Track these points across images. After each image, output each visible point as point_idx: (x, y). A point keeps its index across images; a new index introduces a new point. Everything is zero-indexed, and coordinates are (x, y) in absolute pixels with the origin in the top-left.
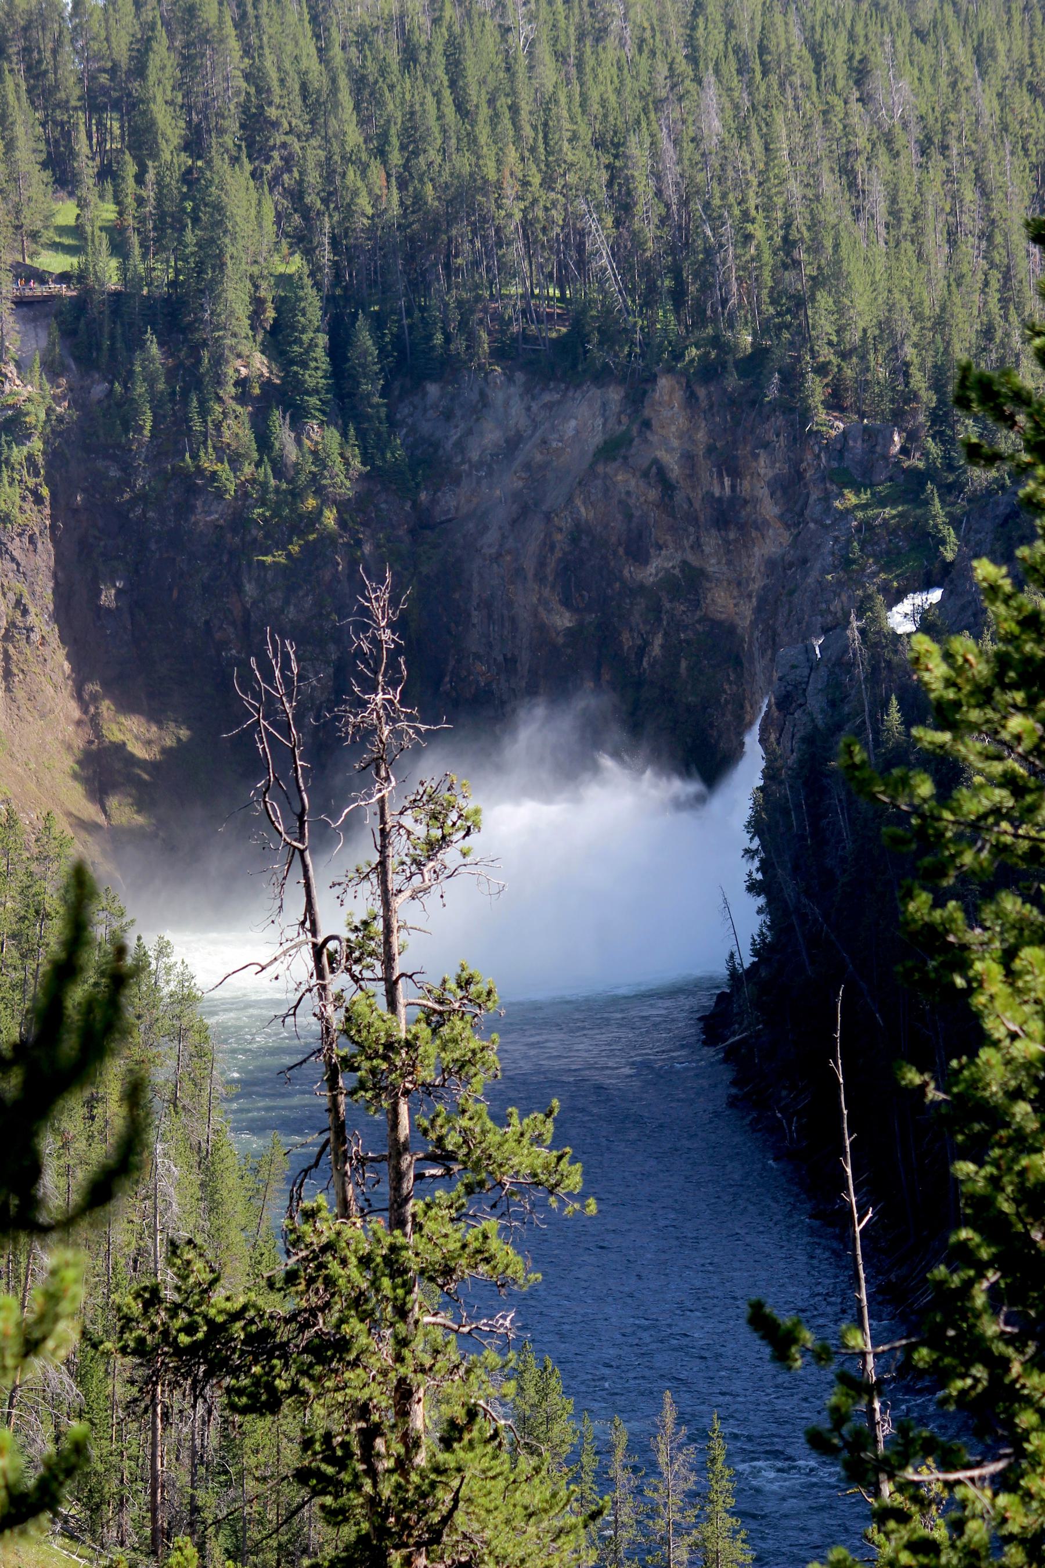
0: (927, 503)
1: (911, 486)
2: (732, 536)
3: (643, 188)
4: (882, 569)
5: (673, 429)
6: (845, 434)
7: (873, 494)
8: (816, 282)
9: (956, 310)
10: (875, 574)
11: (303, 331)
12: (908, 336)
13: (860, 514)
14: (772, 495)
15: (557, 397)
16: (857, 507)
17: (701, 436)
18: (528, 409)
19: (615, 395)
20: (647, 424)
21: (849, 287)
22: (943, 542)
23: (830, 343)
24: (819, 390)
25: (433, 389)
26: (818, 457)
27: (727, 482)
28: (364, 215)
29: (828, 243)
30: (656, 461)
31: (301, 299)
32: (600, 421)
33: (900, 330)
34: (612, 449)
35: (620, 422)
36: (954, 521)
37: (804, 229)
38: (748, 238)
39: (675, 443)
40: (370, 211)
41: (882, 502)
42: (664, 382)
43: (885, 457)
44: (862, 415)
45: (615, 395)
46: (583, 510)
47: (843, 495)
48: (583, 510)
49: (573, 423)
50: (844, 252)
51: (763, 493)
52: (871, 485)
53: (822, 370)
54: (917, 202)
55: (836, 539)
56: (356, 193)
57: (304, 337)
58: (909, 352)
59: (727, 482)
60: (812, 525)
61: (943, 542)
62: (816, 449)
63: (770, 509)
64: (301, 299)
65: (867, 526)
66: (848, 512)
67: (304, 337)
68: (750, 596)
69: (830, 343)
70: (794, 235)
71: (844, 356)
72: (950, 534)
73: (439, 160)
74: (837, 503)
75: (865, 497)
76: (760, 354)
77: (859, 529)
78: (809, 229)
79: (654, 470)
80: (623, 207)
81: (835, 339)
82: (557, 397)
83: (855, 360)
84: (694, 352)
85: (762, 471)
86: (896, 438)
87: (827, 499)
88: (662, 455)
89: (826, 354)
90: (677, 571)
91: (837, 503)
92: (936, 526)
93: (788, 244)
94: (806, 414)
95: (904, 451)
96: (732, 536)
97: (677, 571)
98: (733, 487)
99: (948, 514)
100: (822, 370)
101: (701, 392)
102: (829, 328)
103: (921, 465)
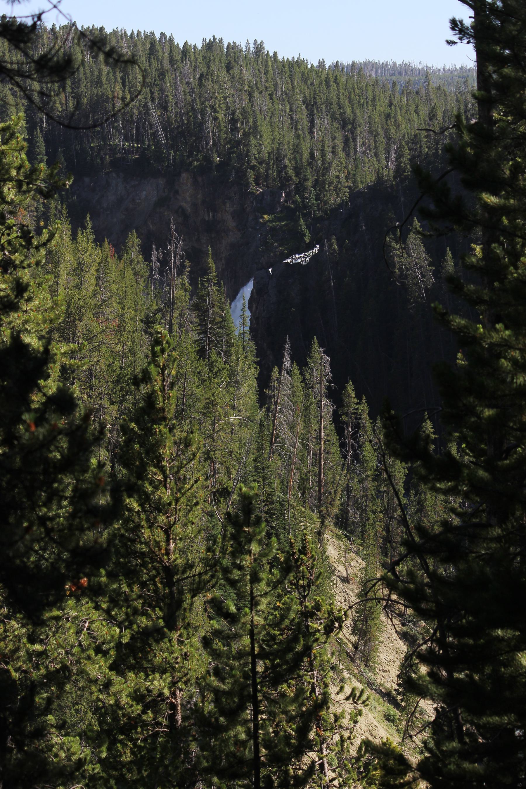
0: (298, 220)
1: (290, 214)
2: (213, 236)
3: (171, 99)
4: (280, 245)
5: (188, 194)
6: (262, 193)
7: (275, 217)
8: (246, 135)
9: (302, 146)
10: (277, 248)
11: (38, 155)
12: (286, 155)
13: (270, 225)
14: (233, 218)
15: (137, 183)
16: (269, 221)
17: (200, 196)
18: (126, 187)
19: (161, 182)
20: (177, 192)
21: (261, 137)
22: (305, 235)
23: (255, 158)
24: (253, 176)
25: (87, 180)
26: (252, 202)
27: (211, 214)
28: (58, 111)
29: (251, 120)
30: (181, 207)
31: (37, 142)
32: (156, 192)
33: (283, 153)
34: (162, 202)
35: (164, 192)
36: (308, 227)
37: (240, 115)
38: (216, 119)
39: (189, 199)
40: (60, 109)
41: (280, 219)
42: (184, 175)
43: (279, 202)
44: (268, 187)
45: (161, 182)
46: (151, 226)
47: (263, 218)
48: (151, 226)
49: (144, 193)
50: (259, 123)
51: (228, 218)
52: (274, 213)
53: (253, 168)
54: (272, 110)
55: (261, 234)
56: (55, 102)
57: (39, 157)
58: (287, 161)
59: (211, 214)
61: (305, 235)
62: (252, 199)
63: (231, 223)
64: (37, 142)
65: (273, 229)
66: (265, 223)
67: (39, 157)
68: (221, 259)
69: (255, 158)
70: (236, 117)
71: (260, 163)
72: (307, 232)
73: (86, 90)
74: (261, 221)
75: (271, 217)
76: (222, 165)
77: (270, 230)
78: (242, 115)
79: (180, 210)
80: (164, 107)
81: (257, 156)
82: (137, 183)
83: (264, 165)
84: (196, 163)
85: (228, 209)
87: (256, 219)
88: (184, 204)
89: (254, 162)
90: (190, 250)
91: (261, 221)
92: (301, 229)
93: (233, 121)
94: (247, 185)
95: (286, 201)
96: (213, 236)
97: (190, 250)
98: (213, 216)
99: (306, 224)
100: (253, 168)
101: (200, 179)
102: (256, 152)
103: (292, 206)
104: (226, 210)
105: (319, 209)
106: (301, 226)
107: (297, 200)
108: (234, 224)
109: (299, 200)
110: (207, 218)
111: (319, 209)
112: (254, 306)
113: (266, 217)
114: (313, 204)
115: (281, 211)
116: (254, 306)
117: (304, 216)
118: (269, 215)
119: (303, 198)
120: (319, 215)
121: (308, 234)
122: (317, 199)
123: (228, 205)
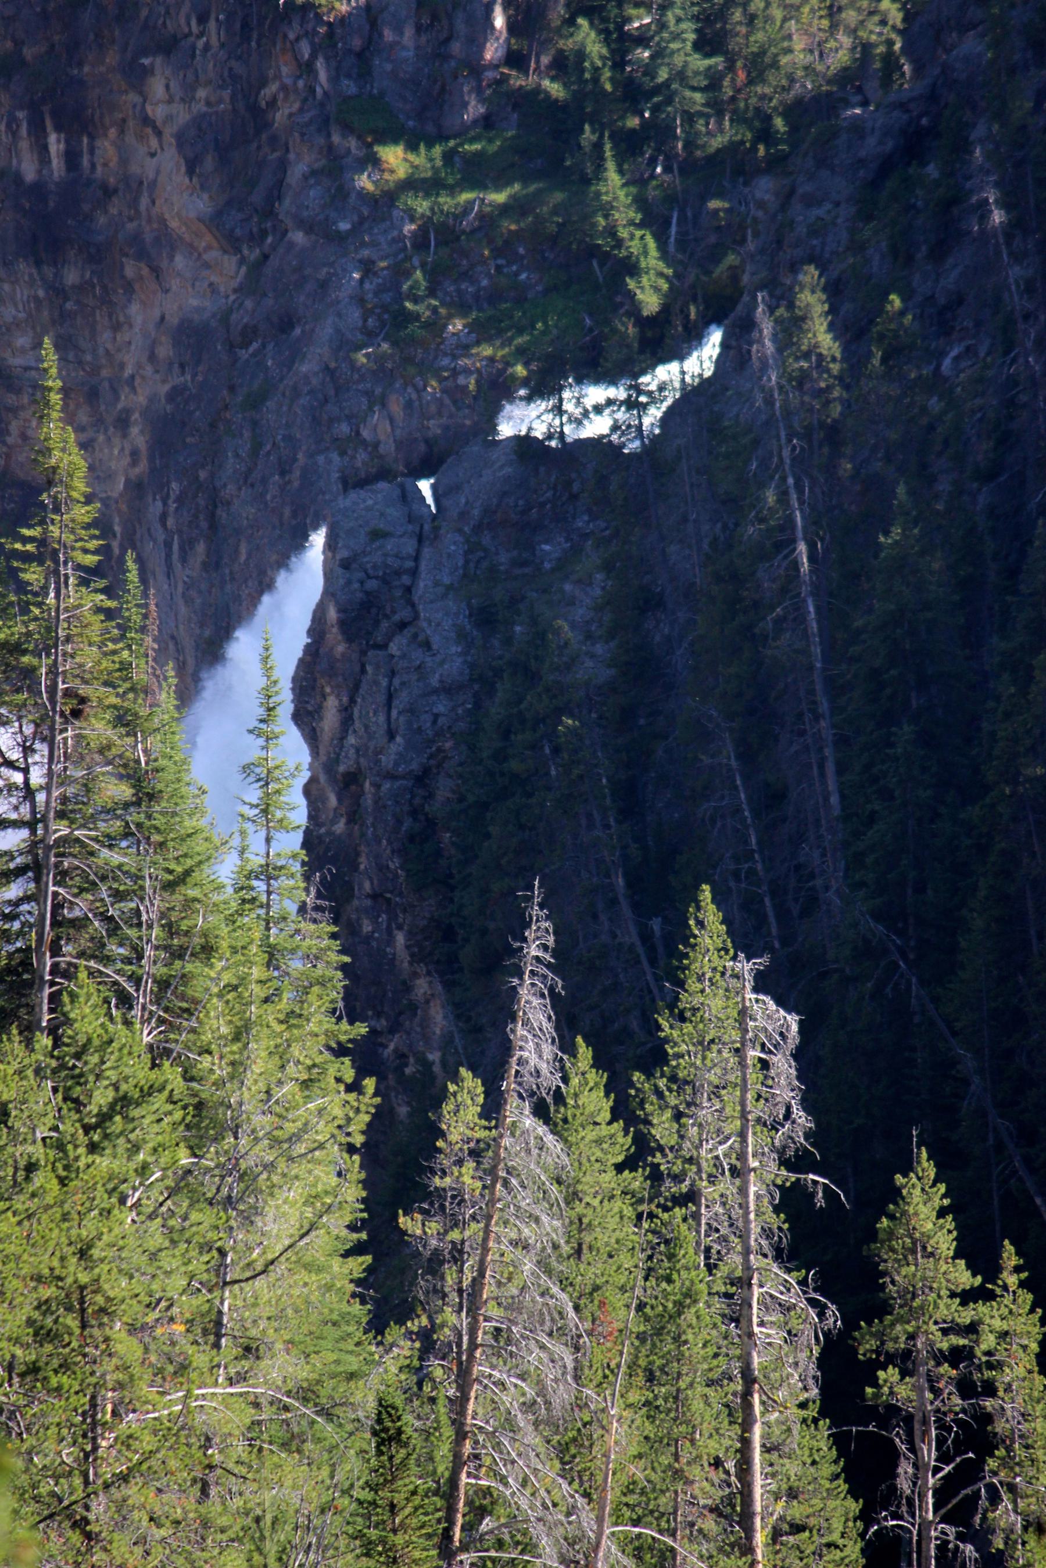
1: (547, 140)
2: (71, 277)
4: (482, 331)
13: (422, 206)
22: (631, 268)
26: (307, 68)
27: (55, 144)
36: (653, 219)
41: (476, 173)
43: (475, 68)
47: (375, 161)
51: (163, 166)
52: (442, 137)
55: (368, 268)
59: (55, 144)
60: (298, 237)
62: (305, 50)
63: (181, 202)
65: (440, 234)
66: (386, 201)
68: (123, 423)
72: (644, 247)
74: (365, 182)
77: (421, 241)
85: (158, 112)
86: (499, 21)
87: (335, 170)
91: (365, 182)
92: (611, 231)
95: (515, 59)
96: (71, 277)
98: (71, 157)
99: (640, 202)
103: (554, 89)
104: (146, 121)
105: (717, 108)
106: (607, 210)
107: (581, 55)
108: (202, 205)
109: (595, 48)
110: (29, 171)
111: (717, 108)
112: (332, 704)
113: (395, 158)
114: (681, 76)
115: (488, 123)
116: (332, 704)
117: (629, 146)
118: (412, 147)
119: (621, 43)
120: (717, 142)
121: (652, 260)
122: (706, 44)
123: (157, 87)
